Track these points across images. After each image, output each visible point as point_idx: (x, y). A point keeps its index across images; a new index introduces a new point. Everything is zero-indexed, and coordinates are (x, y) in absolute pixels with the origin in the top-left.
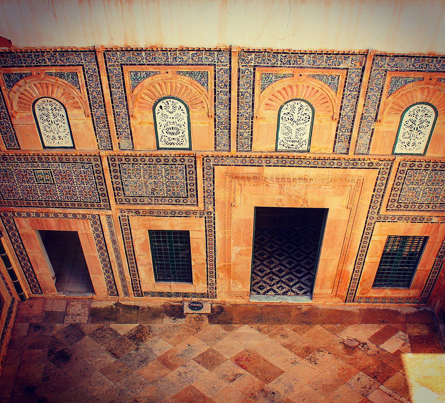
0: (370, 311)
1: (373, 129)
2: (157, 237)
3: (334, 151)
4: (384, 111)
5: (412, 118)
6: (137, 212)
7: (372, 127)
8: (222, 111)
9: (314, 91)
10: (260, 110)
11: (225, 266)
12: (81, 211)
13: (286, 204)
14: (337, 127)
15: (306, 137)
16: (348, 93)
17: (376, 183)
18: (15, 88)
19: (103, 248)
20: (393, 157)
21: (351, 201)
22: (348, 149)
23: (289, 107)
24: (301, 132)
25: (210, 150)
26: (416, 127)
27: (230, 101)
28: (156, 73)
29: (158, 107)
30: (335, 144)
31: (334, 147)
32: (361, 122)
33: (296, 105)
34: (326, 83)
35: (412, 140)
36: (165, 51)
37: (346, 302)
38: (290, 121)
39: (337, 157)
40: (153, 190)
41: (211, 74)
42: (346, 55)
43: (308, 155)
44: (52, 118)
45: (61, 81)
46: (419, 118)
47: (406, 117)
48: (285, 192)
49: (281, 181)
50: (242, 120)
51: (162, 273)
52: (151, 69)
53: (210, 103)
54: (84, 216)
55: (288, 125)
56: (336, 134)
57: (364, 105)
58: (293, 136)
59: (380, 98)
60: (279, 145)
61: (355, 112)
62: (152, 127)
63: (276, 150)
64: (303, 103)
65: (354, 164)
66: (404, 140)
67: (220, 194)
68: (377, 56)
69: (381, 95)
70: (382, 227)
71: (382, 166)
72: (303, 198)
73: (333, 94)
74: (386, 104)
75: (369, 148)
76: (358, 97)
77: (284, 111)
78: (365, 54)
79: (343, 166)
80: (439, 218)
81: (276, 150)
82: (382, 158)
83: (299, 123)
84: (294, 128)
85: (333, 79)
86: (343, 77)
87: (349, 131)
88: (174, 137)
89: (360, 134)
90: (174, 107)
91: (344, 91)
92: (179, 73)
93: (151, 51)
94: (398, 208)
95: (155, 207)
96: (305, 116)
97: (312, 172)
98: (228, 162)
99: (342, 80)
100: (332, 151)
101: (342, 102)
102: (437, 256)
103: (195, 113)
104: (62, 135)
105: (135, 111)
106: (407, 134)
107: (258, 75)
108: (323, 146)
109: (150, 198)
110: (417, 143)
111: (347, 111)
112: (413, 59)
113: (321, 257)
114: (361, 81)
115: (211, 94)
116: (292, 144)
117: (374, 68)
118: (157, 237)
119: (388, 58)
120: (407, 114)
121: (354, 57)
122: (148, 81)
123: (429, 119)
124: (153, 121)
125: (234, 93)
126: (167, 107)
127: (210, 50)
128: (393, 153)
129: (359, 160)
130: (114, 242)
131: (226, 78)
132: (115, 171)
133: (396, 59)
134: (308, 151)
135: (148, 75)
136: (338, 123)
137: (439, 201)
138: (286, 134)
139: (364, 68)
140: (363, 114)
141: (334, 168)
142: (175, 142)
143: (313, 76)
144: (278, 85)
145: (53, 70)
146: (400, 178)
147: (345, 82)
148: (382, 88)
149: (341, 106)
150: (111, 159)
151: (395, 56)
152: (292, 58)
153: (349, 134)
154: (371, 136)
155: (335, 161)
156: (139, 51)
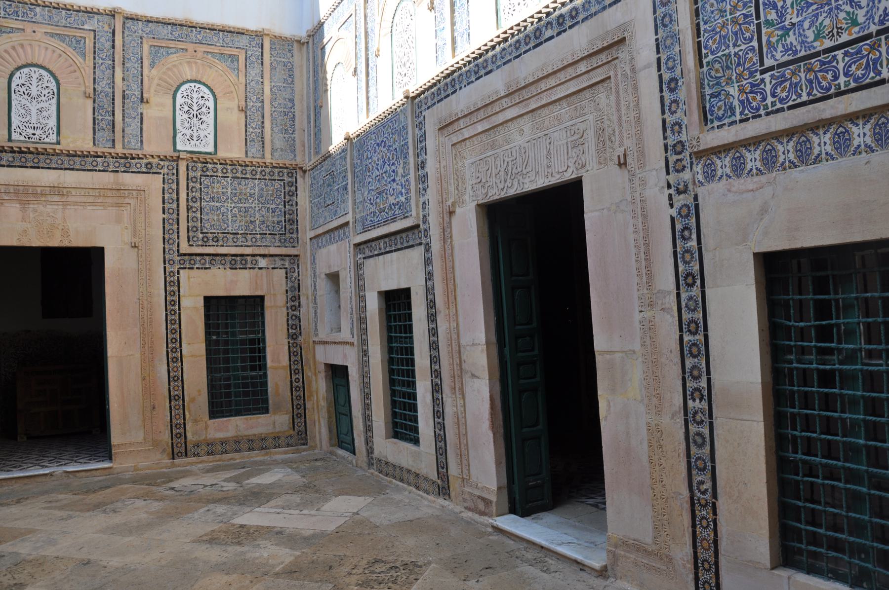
1: (142, 114)
3: (94, 144)
4: (149, 88)
5: (187, 100)
7: (140, 111)
9: (56, 55)
13: (36, 241)
14: (94, 108)
15: (53, 122)
16: (101, 61)
17: (163, 198)
20: (176, 154)
21: (135, 233)
22: (114, 141)
23: (24, 75)
24: (44, 114)
26: (195, 113)
30: (94, 133)
31: (94, 138)
32: (124, 103)
33: (32, 74)
34: (70, 46)
35: (195, 131)
37: (173, 458)
38: (26, 97)
39: (100, 150)
42: (90, 12)
43: (58, 147)
46: (195, 101)
47: (179, 100)
48: (32, 215)
55: (24, 102)
56: (94, 118)
57: (123, 79)
58: (34, 120)
59: (142, 72)
60: (13, 134)
61: (113, 87)
63: (10, 140)
65: (127, 162)
66: (184, 131)
68: (127, 18)
69: (142, 67)
70: (192, 280)
71: (166, 171)
72: (60, 227)
73: (81, 61)
74: (151, 79)
75: (142, 141)
76: (114, 67)
78: (113, 14)
79: (111, 168)
80: (266, 259)
81: (10, 140)
82: (162, 153)
83: (40, 100)
84: (34, 107)
85: (78, 42)
86: (90, 40)
87: (111, 114)
89: (126, 120)
91: (94, 58)
94: (205, 243)
96: (47, 91)
97: (69, 178)
99: (89, 43)
100: (92, 143)
101: (94, 73)
102: (289, 335)
106: (186, 123)
108: (79, 138)
110: (202, 136)
111: (102, 85)
112: (170, 27)
113: (109, 354)
114: (113, 47)
116: (33, 131)
117: (126, 33)
119: (140, 23)
120: (179, 95)
121: (100, 17)
123: (207, 102)
128: (175, 150)
129: (133, 158)
133: (150, 24)
134: (58, 143)
136: (94, 102)
137: (258, 229)
138: (23, 116)
139: (114, 31)
140: (124, 91)
141: (100, 171)
143: (52, 35)
146: (194, 190)
147: (95, 47)
148: (142, 59)
149: (94, 79)
151: (149, 21)
153: (111, 118)
154: (142, 124)
155: (99, 160)
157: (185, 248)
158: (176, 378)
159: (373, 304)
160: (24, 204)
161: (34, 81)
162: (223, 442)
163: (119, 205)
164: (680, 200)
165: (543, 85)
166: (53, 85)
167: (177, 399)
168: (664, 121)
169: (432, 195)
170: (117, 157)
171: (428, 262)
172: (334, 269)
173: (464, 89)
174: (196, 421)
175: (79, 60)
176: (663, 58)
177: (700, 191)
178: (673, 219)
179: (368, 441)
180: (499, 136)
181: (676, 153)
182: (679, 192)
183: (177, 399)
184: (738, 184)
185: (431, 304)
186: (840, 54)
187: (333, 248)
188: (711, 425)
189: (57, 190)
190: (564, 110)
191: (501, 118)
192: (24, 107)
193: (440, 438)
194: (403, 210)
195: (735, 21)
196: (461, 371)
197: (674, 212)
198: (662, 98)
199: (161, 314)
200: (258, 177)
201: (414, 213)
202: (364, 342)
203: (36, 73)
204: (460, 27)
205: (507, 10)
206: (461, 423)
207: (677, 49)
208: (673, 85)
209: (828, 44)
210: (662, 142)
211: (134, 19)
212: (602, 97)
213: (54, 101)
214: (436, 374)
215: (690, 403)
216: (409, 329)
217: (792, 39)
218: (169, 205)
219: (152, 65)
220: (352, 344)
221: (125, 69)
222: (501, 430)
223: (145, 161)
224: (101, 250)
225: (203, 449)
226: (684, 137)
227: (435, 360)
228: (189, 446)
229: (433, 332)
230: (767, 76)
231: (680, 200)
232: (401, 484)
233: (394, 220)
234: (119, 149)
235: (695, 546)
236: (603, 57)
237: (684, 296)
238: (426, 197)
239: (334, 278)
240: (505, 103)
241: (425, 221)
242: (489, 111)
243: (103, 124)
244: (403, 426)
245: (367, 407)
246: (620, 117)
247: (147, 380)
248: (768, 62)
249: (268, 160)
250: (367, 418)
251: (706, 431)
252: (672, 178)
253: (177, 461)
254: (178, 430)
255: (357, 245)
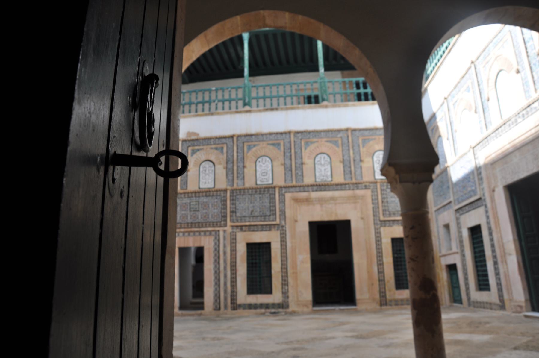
2: (252, 247)
6: (241, 228)
8: (288, 162)
10: (306, 160)
11: (293, 273)
12: (210, 229)
15: (329, 173)
18: (195, 156)
19: (217, 261)
25: (282, 184)
27: (291, 156)
28: (258, 145)
29: (258, 162)
36: (262, 135)
40: (252, 211)
41: (282, 144)
42: (339, 131)
44: (207, 172)
45: (216, 151)
49: (321, 201)
50: (298, 165)
51: (252, 289)
52: (256, 143)
53: (281, 158)
54: (210, 232)
62: (254, 172)
64: (325, 156)
65: (357, 185)
67: (289, 212)
77: (317, 160)
78: (347, 130)
84: (323, 169)
88: (265, 177)
90: (266, 161)
92: (268, 144)
93: (256, 135)
94: (390, 215)
95: (253, 223)
97: (337, 194)
98: (291, 190)
99: (340, 142)
103: (275, 163)
104: (210, 181)
105: (247, 164)
107: (303, 143)
108: (339, 179)
109: (249, 217)
111: (346, 157)
114: (348, 142)
115: (282, 153)
118: (252, 247)
122: (254, 149)
124: (254, 169)
125: (293, 151)
126: (262, 161)
127: (281, 133)
130: (225, 253)
131: (288, 145)
132: (233, 200)
135: (255, 146)
142: (265, 180)
143: (327, 141)
144: (312, 147)
145: (214, 146)
150: (232, 191)
152: (316, 133)
156: (251, 135)
157: (382, 218)
158: (381, 272)
159: (465, 234)
160: (321, 205)
161: (322, 159)
162: (402, 300)
163: (355, 203)
166: (329, 160)
167: (382, 281)
169: (485, 185)
170: (353, 184)
171: (487, 212)
172: (446, 222)
174: (390, 291)
175: (337, 149)
179: (468, 294)
183: (382, 281)
185: (490, 229)
187: (445, 213)
189: (333, 199)
192: (320, 169)
193: (499, 284)
194: (474, 192)
196: (504, 254)
199: (374, 246)
201: (479, 193)
202: (462, 251)
203: (322, 156)
204: (488, 120)
206: (507, 275)
211: (354, 130)
213: (329, 166)
214: (495, 257)
216: (482, 242)
218: (374, 200)
219: (363, 146)
220: (457, 253)
221: (353, 150)
222: (524, 276)
223: (364, 185)
224: (347, 223)
225: (393, 303)
227: (494, 251)
228: (388, 301)
229: (492, 240)
233: (471, 197)
234: (354, 181)
239: (447, 227)
241: (484, 195)
243: (347, 172)
244: (483, 284)
245: (466, 279)
247: (370, 272)
250: (467, 284)
254: (383, 294)
255: (457, 210)
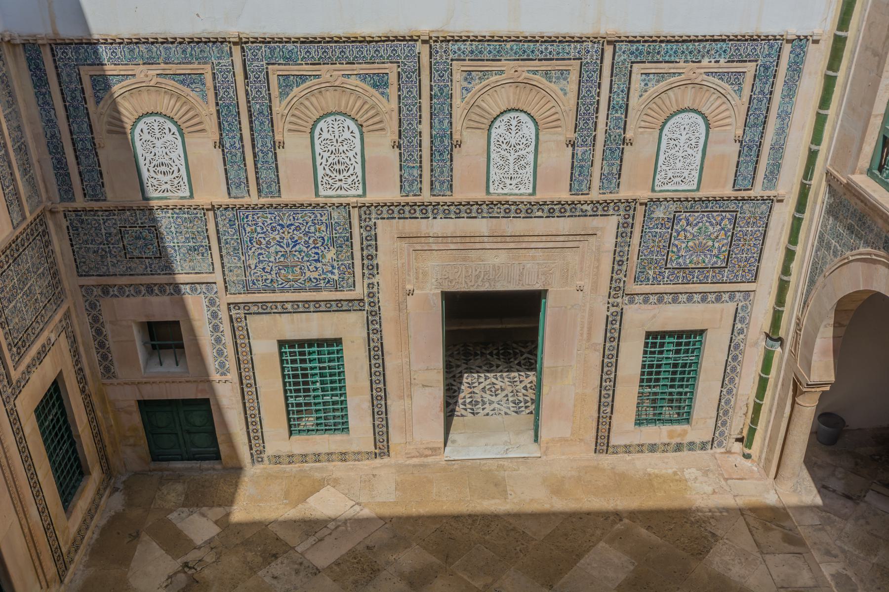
0: (97, 552)
158: (43, 510)
164: (612, 309)
165: (526, 239)
168: (612, 277)
173: (438, 220)
176: (618, 250)
177: (625, 307)
178: (608, 317)
180: (473, 254)
181: (616, 289)
182: (613, 306)
184: (643, 306)
186: (697, 271)
188: (614, 391)
190: (539, 253)
191: (478, 246)
195: (658, 247)
197: (609, 314)
198: (613, 267)
200: (26, 245)
205: (497, 183)
207: (627, 248)
208: (620, 263)
209: (693, 266)
210: (609, 285)
212: (569, 254)
215: (604, 384)
217: (681, 260)
226: (621, 285)
230: (667, 271)
231: (612, 309)
232: (318, 464)
233: (317, 289)
235: (597, 432)
236: (578, 238)
237: (608, 345)
238: (375, 280)
240: (486, 239)
242: (468, 240)
246: (582, 268)
248: (669, 266)
249: (30, 218)
251: (611, 392)
252: (611, 300)
253: (66, 580)
